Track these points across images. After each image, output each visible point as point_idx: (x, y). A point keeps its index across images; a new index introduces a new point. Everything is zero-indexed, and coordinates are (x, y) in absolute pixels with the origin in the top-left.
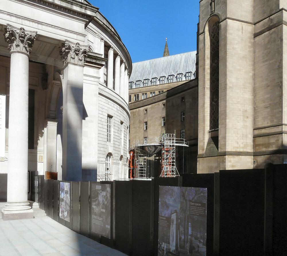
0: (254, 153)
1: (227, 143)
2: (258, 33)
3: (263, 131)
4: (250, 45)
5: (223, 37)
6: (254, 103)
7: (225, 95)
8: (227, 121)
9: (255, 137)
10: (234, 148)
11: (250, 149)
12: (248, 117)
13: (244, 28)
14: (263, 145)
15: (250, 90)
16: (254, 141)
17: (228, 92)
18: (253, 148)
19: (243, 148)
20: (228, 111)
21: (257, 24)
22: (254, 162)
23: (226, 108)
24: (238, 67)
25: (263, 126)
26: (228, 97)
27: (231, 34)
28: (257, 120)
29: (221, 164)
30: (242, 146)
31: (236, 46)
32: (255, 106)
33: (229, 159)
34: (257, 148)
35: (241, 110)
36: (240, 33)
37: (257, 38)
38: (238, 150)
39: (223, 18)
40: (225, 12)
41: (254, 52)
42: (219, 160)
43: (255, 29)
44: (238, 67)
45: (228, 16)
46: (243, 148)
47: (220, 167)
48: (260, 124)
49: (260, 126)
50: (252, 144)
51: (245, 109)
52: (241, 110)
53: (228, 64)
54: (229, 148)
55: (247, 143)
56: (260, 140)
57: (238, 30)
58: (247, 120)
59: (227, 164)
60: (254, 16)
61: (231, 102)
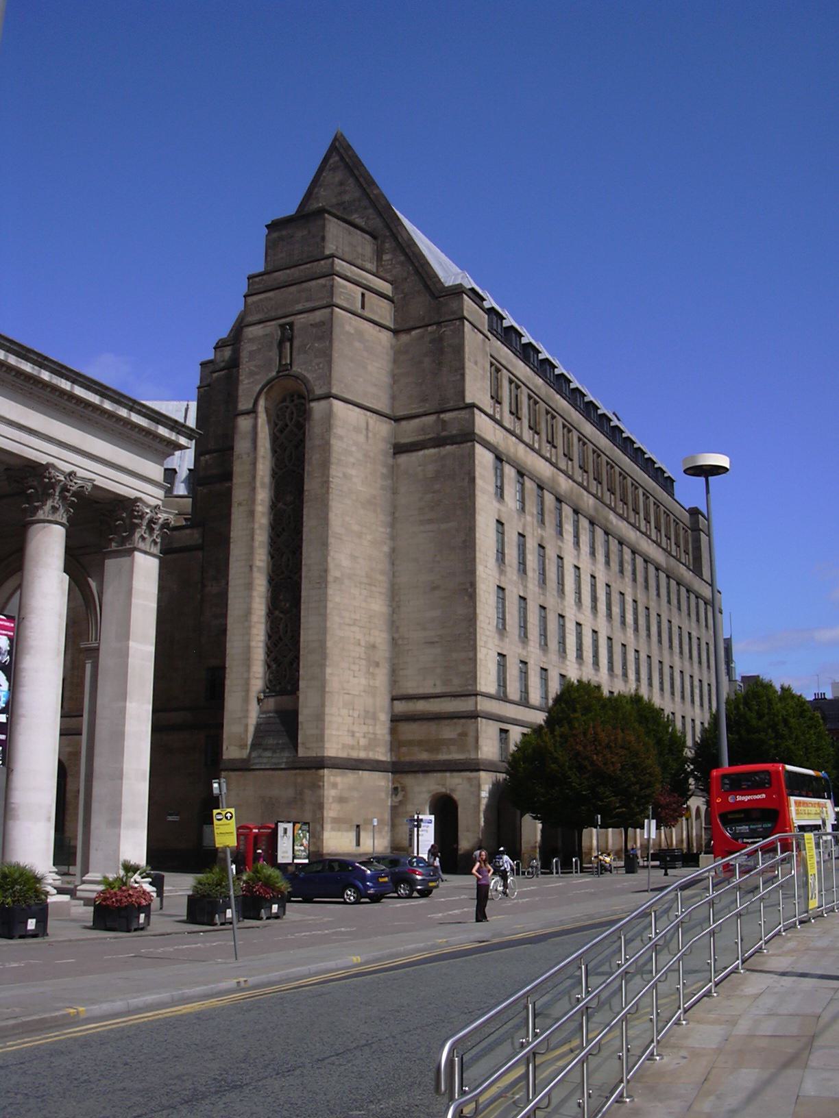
0: (394, 764)
1: (327, 732)
3: (421, 706)
4: (384, 471)
5: (317, 442)
6: (393, 625)
7: (323, 600)
8: (328, 670)
9: (396, 720)
10: (344, 746)
11: (382, 754)
12: (377, 665)
13: (371, 427)
14: (420, 743)
15: (384, 591)
16: (393, 731)
17: (330, 592)
18: (391, 750)
19: (366, 748)
20: (329, 644)
21: (404, 423)
22: (395, 790)
24: (356, 528)
25: (421, 691)
26: (330, 605)
27: (341, 438)
28: (401, 673)
29: (307, 792)
30: (363, 742)
31: (353, 472)
32: (396, 636)
33: (332, 779)
34: (404, 749)
35: (363, 643)
36: (362, 438)
37: (403, 459)
38: (354, 754)
39: (319, 392)
40: (327, 378)
41: (395, 492)
42: (299, 780)
44: (356, 528)
45: (334, 391)
46: (366, 748)
48: (411, 687)
49: (411, 692)
50: (388, 738)
51: (372, 640)
52: (363, 643)
53: (332, 516)
54: (332, 750)
55: (374, 734)
56: (411, 731)
57: (357, 430)
58: (377, 671)
59: (326, 793)
60: (393, 398)
61: (337, 619)
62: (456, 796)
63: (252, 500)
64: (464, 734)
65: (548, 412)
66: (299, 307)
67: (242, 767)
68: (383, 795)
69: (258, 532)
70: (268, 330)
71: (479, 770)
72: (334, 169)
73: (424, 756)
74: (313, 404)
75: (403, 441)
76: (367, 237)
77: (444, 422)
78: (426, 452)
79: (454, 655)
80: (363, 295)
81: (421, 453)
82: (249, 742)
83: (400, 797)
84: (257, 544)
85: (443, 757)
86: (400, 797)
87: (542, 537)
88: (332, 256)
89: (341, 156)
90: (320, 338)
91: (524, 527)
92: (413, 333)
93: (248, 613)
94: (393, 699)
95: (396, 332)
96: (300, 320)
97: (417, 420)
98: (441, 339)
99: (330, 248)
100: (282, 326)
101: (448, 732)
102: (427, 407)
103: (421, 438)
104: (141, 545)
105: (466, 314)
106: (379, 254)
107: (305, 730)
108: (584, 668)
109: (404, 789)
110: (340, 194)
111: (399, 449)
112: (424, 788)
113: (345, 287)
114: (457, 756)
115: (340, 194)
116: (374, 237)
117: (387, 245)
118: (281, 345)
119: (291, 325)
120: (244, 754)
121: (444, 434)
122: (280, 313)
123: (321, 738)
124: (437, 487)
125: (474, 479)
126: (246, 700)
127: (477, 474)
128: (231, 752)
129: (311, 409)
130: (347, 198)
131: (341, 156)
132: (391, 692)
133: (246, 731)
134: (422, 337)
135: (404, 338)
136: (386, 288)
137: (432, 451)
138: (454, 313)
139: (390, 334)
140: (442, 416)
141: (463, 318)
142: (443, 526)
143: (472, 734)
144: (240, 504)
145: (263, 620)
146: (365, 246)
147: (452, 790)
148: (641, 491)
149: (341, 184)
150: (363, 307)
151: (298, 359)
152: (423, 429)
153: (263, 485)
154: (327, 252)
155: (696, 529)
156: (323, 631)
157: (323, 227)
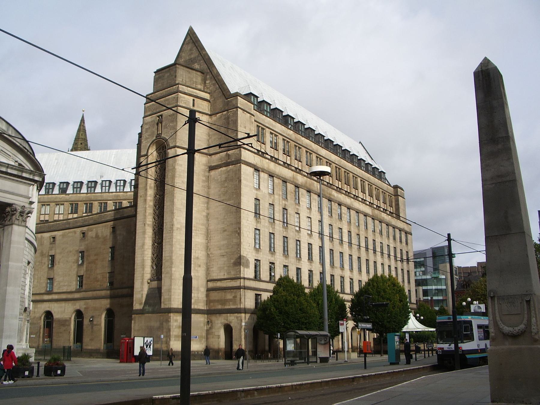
0: (207, 310)
1: (172, 297)
2: (214, 166)
3: (219, 284)
4: (204, 179)
5: (170, 168)
7: (171, 238)
8: (173, 269)
9: (209, 290)
12: (200, 266)
16: (207, 296)
17: (174, 234)
20: (174, 258)
21: (213, 156)
22: (208, 322)
23: (172, 253)
25: (219, 278)
26: (174, 240)
29: (164, 324)
33: (175, 318)
34: (212, 304)
37: (213, 173)
39: (171, 145)
41: (209, 188)
42: (162, 318)
43: (209, 162)
47: (162, 327)
48: (215, 275)
49: (215, 278)
50: (205, 299)
53: (176, 200)
55: (198, 297)
56: (215, 295)
58: (199, 269)
59: (171, 324)
61: (178, 246)
62: (232, 325)
63: (146, 194)
64: (235, 297)
65: (296, 146)
67: (141, 312)
68: (202, 325)
69: (148, 208)
70: (153, 119)
71: (241, 313)
72: (188, 44)
73: (220, 307)
74: (169, 151)
75: (213, 165)
76: (199, 73)
77: (229, 155)
78: (222, 169)
80: (193, 100)
81: (220, 170)
82: (143, 302)
83: (210, 326)
84: (147, 214)
85: (227, 307)
86: (210, 326)
87: (285, 205)
88: (178, 84)
89: (192, 38)
90: (172, 121)
91: (273, 201)
92: (218, 115)
93: (143, 244)
94: (208, 281)
95: (210, 115)
97: (218, 155)
98: (228, 118)
99: (179, 80)
100: (158, 116)
103: (220, 163)
104: (17, 222)
105: (239, 105)
106: (204, 81)
107: (164, 296)
108: (313, 264)
109: (211, 322)
110: (190, 55)
111: (212, 168)
112: (219, 321)
113: (184, 98)
115: (190, 55)
116: (203, 73)
117: (208, 76)
118: (157, 124)
119: (161, 116)
120: (141, 307)
121: (229, 161)
122: (158, 110)
123: (170, 299)
124: (226, 185)
125: (240, 181)
126: (142, 283)
127: (242, 178)
128: (137, 306)
129: (168, 153)
130: (193, 56)
131: (192, 38)
132: (207, 278)
133: (142, 297)
135: (214, 118)
136: (207, 96)
137: (224, 168)
138: (234, 105)
139: (207, 117)
140: (228, 152)
141: (237, 107)
143: (238, 297)
145: (151, 247)
146: (197, 77)
147: (230, 322)
148: (359, 179)
149: (191, 50)
150: (193, 106)
151: (164, 131)
152: (221, 159)
153: (151, 188)
154: (177, 82)
155: (396, 195)
156: (172, 252)
157: (176, 72)
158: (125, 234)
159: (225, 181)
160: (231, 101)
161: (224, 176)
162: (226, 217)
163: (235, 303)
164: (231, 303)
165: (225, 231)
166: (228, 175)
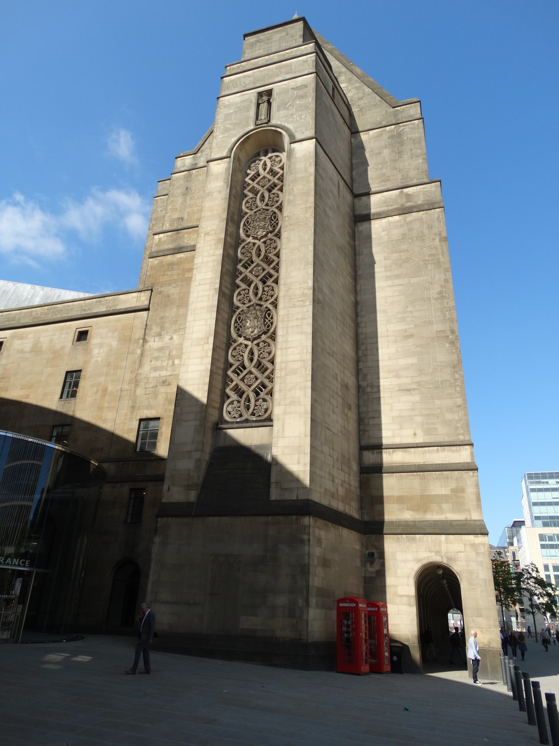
62: (456, 568)
64: (459, 491)
66: (277, 79)
70: (246, 97)
79: (438, 402)
85: (433, 516)
96: (276, 88)
98: (400, 135)
101: (438, 486)
102: (389, 185)
103: (386, 208)
114: (450, 515)
120: (192, 496)
121: (409, 204)
134: (381, 135)
137: (397, 218)
140: (405, 190)
142: (413, 281)
143: (470, 490)
144: (207, 234)
147: (449, 559)
158: (114, 344)
159: (404, 237)
160: (403, 111)
161: (396, 233)
162: (409, 309)
163: (459, 506)
164: (445, 506)
165: (411, 336)
166: (410, 230)
